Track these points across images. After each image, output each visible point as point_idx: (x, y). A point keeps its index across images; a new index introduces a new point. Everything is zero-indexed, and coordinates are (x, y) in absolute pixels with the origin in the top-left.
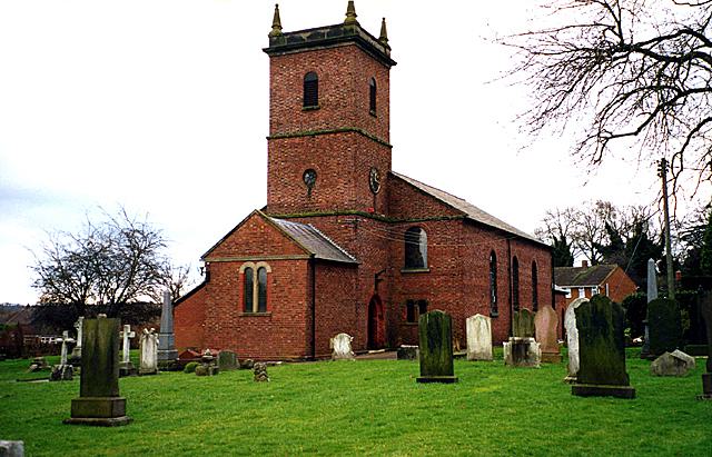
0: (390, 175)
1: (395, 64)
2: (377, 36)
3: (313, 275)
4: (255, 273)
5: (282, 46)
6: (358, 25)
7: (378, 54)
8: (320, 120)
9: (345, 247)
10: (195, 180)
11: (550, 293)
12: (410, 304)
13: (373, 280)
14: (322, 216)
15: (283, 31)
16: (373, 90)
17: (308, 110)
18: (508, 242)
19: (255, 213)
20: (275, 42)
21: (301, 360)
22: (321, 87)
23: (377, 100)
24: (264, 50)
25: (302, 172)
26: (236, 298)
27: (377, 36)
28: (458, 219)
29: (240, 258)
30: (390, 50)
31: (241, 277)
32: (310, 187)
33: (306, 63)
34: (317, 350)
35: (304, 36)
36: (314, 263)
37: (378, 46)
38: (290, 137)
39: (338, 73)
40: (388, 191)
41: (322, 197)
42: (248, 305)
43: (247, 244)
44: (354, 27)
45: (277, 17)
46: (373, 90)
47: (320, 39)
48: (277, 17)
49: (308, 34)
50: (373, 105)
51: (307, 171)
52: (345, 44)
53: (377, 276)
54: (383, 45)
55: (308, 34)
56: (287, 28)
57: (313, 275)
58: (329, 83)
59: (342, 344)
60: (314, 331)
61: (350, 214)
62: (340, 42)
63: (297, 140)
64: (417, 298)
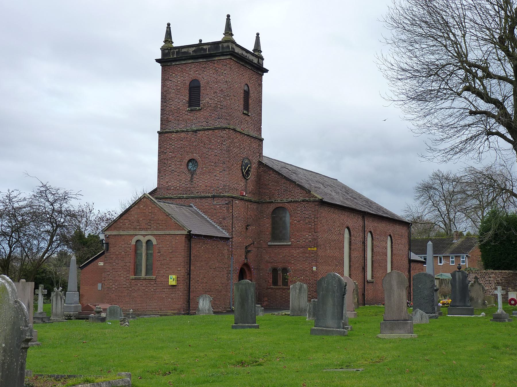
0: (260, 163)
1: (266, 71)
2: (251, 48)
3: (190, 249)
4: (144, 245)
5: (172, 57)
6: (234, 42)
7: (252, 64)
8: (198, 120)
9: (220, 224)
10: (107, 157)
11: (406, 262)
12: (275, 271)
13: (243, 251)
14: (201, 198)
15: (174, 45)
16: (247, 94)
17: (192, 110)
18: (363, 217)
19: (144, 197)
20: (168, 54)
21: (179, 314)
22: (202, 91)
23: (251, 102)
24: (157, 61)
25: (187, 159)
26: (128, 264)
27: (251, 48)
28: (314, 201)
29: (132, 232)
30: (263, 59)
31: (133, 248)
32: (193, 173)
33: (191, 72)
34: (189, 308)
35: (191, 50)
36: (190, 236)
37: (251, 57)
38: (177, 132)
39: (217, 79)
40: (259, 177)
41: (203, 182)
42: (136, 270)
43: (138, 222)
44: (230, 45)
45: (169, 34)
46: (247, 94)
47: (202, 53)
48: (169, 34)
49: (194, 49)
50: (246, 106)
51: (190, 161)
52: (222, 58)
53: (246, 247)
54: (256, 56)
55: (194, 49)
56: (176, 43)
57: (190, 249)
58: (210, 83)
59: (204, 304)
60: (189, 292)
61: (224, 197)
62: (219, 56)
63: (183, 135)
64: (280, 266)
